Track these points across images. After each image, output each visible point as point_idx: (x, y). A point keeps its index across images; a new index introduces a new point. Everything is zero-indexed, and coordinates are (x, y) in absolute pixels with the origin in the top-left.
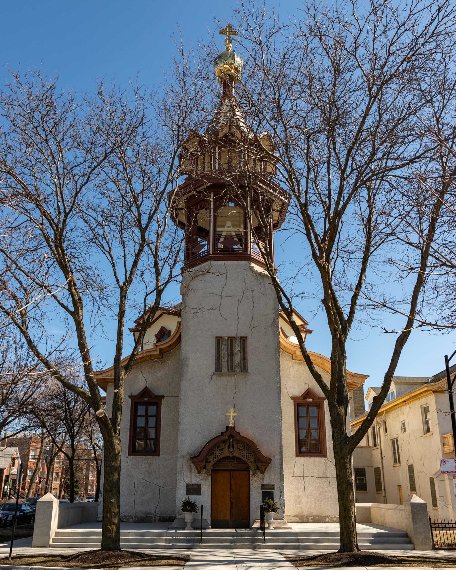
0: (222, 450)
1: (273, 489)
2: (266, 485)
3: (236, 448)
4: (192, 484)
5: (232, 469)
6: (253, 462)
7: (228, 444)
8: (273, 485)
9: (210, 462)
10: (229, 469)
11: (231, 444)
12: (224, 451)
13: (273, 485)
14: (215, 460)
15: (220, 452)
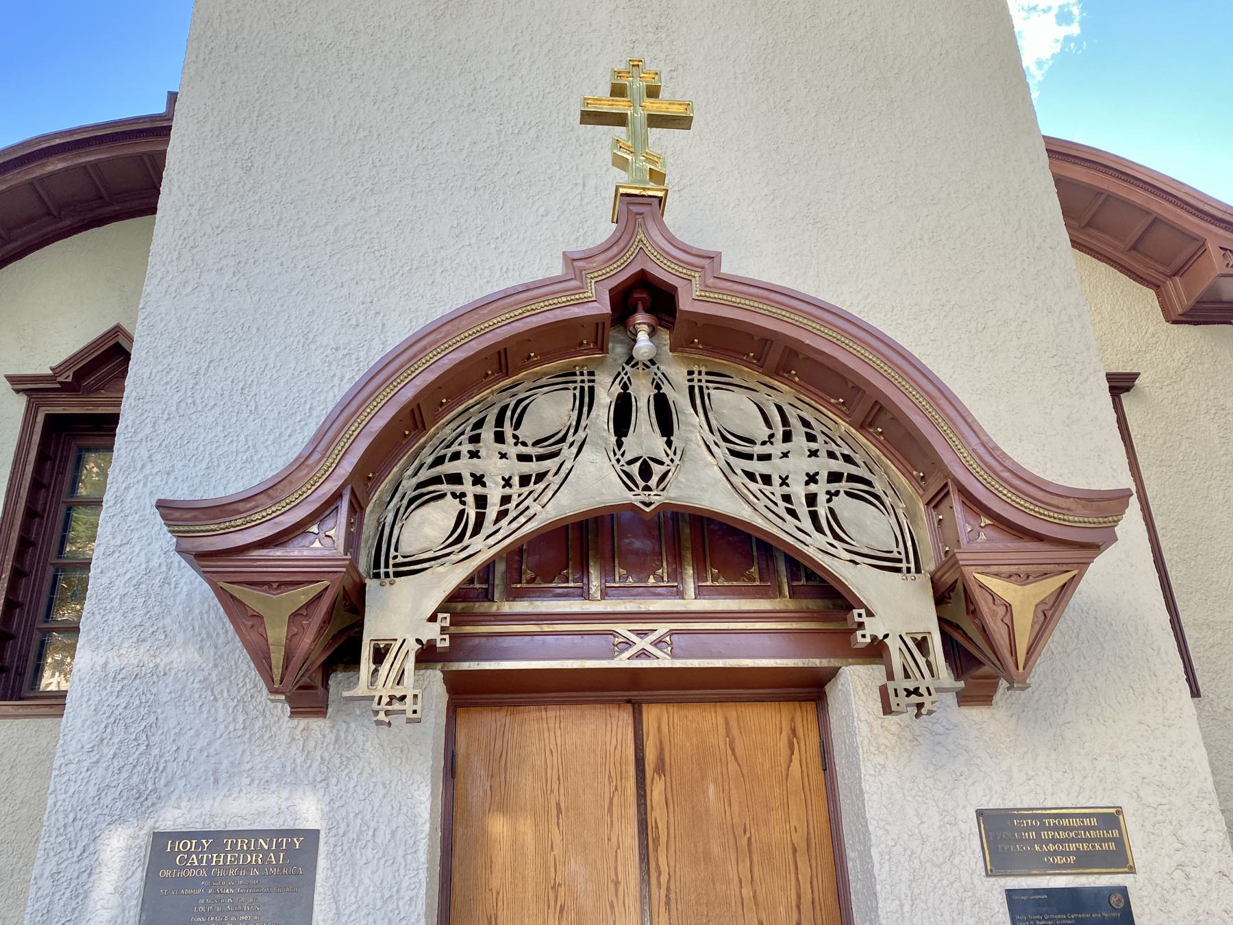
0: (550, 446)
1: (1119, 858)
2: (1039, 817)
3: (689, 423)
4: (217, 839)
5: (665, 662)
6: (887, 563)
7: (606, 397)
8: (1111, 820)
9: (410, 568)
10: (622, 661)
11: (642, 394)
12: (567, 452)
13: (1111, 820)
14: (477, 543)
15: (533, 468)
